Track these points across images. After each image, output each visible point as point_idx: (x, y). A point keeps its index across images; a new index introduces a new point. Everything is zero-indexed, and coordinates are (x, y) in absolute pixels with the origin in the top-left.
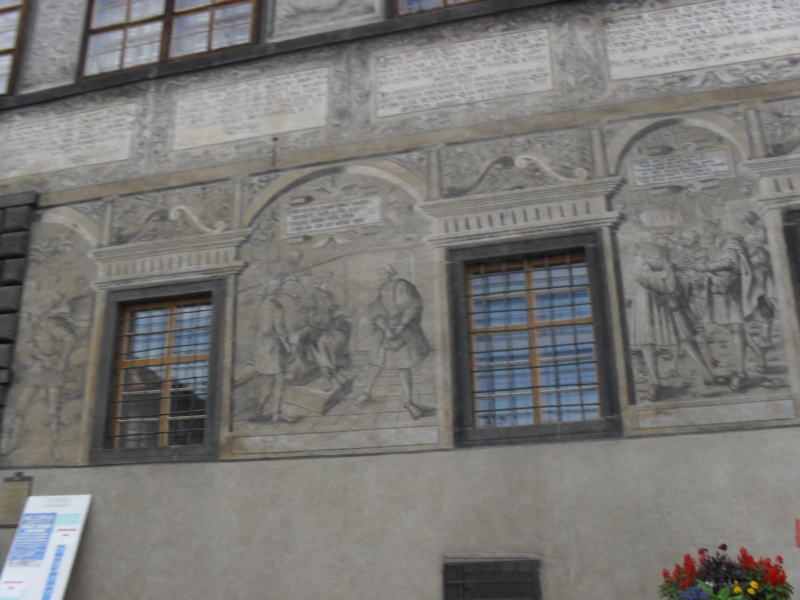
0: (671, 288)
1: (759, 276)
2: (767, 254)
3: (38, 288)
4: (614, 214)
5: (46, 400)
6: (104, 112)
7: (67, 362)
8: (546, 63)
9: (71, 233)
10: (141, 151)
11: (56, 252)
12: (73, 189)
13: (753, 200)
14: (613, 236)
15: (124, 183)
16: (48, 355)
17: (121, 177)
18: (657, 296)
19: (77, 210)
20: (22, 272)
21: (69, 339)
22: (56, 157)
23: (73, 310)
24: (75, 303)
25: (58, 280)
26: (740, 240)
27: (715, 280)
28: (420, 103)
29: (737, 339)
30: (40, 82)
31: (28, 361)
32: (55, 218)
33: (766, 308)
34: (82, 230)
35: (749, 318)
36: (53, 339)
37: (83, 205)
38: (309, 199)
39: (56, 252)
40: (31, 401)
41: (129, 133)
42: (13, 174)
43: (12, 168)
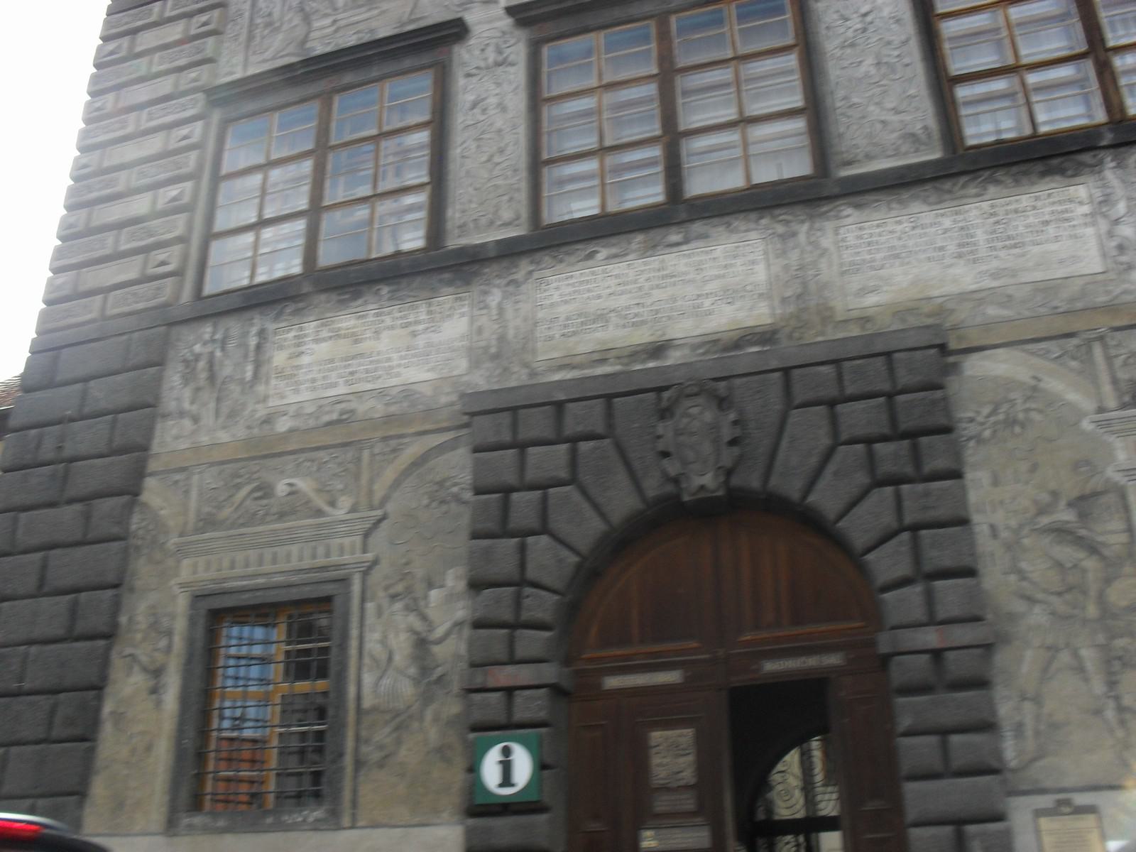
3: (996, 482)
5: (1080, 669)
6: (1025, 201)
7: (1101, 599)
9: (1034, 391)
10: (1124, 259)
11: (1011, 422)
12: (1010, 321)
15: (1111, 308)
16: (1059, 594)
17: (1102, 299)
19: (1033, 354)
20: (958, 456)
21: (1091, 564)
22: (951, 271)
23: (1083, 516)
24: (1084, 503)
25: (1034, 468)
30: (869, 157)
31: (1019, 606)
34: (1054, 385)
36: (1059, 565)
37: (1043, 345)
39: (1011, 422)
40: (1045, 672)
41: (1090, 231)
42: (871, 300)
43: (864, 291)
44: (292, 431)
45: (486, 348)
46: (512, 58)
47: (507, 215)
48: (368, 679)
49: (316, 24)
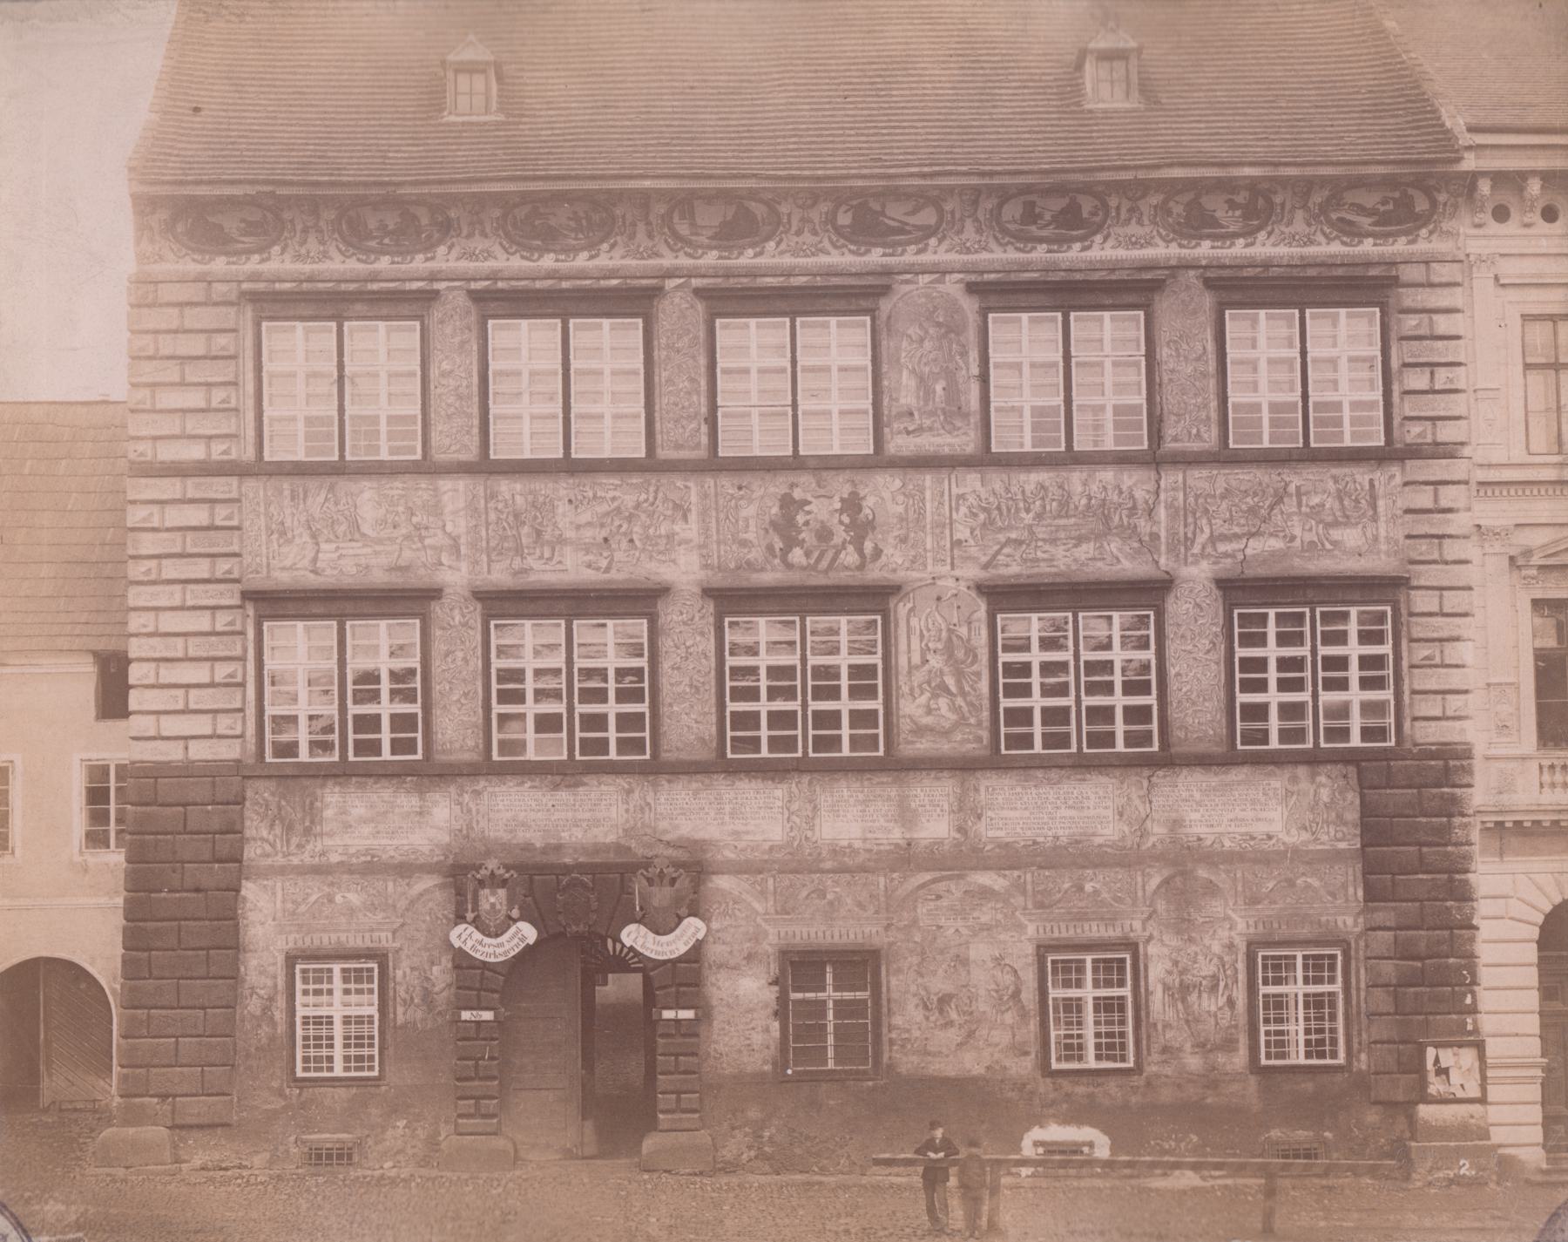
0: (1177, 984)
1: (1230, 982)
2: (1236, 970)
4: (1147, 934)
8: (1109, 813)
10: (792, 834)
13: (1233, 933)
14: (1145, 948)
18: (1166, 988)
26: (1221, 958)
27: (1204, 983)
28: (1019, 830)
29: (1212, 1021)
32: (723, 882)
33: (1231, 1003)
35: (1220, 1009)
38: (939, 897)
44: (341, 863)
45: (461, 831)
46: (471, 622)
47: (470, 743)
48: (400, 1010)
49: (324, 546)
